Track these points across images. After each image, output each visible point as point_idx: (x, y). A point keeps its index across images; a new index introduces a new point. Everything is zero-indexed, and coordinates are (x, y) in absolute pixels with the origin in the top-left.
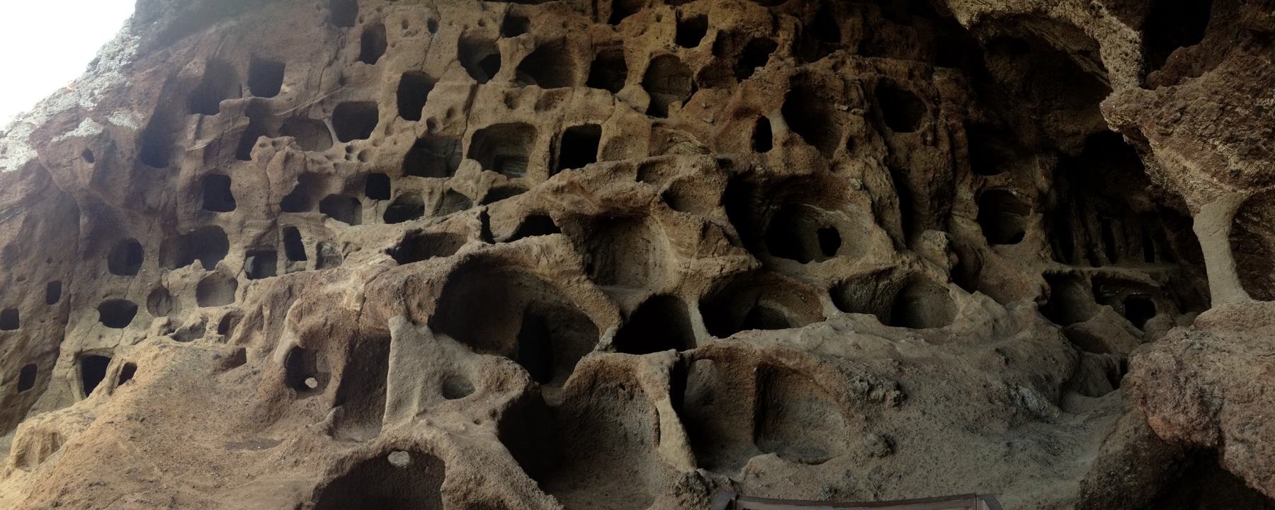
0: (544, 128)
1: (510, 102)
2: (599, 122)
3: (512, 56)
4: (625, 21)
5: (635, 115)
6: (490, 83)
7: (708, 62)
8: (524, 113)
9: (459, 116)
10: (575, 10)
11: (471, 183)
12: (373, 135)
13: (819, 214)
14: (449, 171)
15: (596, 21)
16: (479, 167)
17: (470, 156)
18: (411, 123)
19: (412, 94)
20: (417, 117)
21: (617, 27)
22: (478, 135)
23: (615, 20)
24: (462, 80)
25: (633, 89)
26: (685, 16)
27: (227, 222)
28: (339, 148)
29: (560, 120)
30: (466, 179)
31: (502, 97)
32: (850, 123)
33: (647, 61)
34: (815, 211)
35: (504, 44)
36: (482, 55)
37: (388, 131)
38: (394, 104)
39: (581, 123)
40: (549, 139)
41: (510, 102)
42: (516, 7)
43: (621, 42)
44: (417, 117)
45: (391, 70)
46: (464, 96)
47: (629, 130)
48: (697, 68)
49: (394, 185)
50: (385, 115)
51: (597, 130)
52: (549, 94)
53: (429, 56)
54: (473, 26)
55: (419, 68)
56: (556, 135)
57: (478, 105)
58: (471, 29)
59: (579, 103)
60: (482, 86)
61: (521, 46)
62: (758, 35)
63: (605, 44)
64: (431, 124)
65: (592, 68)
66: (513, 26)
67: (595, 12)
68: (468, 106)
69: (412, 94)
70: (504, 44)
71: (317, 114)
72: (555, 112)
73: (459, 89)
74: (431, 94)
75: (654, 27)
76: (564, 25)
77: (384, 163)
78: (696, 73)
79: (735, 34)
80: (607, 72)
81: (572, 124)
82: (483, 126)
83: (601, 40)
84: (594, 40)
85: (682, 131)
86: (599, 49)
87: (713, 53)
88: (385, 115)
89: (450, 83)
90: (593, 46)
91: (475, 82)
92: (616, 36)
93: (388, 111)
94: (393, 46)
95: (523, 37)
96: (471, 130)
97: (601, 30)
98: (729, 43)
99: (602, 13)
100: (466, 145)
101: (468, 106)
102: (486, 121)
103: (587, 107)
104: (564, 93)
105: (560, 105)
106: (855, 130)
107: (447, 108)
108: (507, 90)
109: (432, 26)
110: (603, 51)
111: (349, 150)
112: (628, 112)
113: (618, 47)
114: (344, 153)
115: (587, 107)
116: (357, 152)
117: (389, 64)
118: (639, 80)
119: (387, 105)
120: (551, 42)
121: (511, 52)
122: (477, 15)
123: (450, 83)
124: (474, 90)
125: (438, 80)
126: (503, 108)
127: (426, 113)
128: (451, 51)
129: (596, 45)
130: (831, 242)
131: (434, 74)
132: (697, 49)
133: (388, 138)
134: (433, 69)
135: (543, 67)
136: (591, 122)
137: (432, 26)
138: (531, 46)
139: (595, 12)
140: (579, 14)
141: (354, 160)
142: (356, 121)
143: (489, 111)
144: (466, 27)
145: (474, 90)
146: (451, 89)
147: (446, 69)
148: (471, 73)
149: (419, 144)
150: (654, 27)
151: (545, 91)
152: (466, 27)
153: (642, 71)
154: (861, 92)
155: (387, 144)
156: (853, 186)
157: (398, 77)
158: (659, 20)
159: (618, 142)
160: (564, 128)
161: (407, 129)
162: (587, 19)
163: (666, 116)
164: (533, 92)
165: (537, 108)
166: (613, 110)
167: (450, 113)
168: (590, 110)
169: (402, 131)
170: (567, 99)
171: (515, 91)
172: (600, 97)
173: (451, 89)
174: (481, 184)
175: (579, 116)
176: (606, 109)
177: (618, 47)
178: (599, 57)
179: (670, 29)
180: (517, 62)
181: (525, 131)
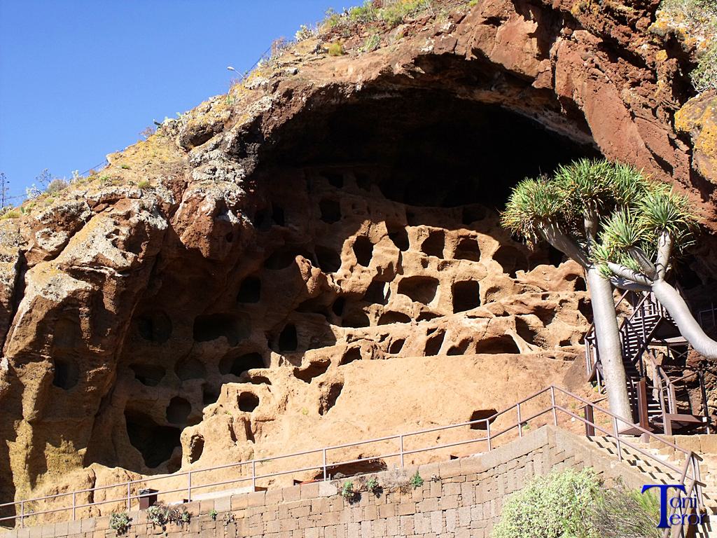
8: (431, 271)
18: (365, 268)
24: (391, 245)
41: (425, 264)
46: (397, 257)
47: (499, 284)
59: (463, 269)
60: (402, 252)
73: (393, 253)
77: (354, 290)
78: (527, 258)
85: (530, 286)
86: (461, 239)
89: (385, 248)
94: (345, 218)
96: (399, 278)
102: (408, 274)
126: (420, 266)
127: (373, 264)
136: (473, 279)
143: (412, 269)
147: (381, 239)
159: (493, 290)
164: (434, 261)
167: (391, 264)
169: (362, 272)
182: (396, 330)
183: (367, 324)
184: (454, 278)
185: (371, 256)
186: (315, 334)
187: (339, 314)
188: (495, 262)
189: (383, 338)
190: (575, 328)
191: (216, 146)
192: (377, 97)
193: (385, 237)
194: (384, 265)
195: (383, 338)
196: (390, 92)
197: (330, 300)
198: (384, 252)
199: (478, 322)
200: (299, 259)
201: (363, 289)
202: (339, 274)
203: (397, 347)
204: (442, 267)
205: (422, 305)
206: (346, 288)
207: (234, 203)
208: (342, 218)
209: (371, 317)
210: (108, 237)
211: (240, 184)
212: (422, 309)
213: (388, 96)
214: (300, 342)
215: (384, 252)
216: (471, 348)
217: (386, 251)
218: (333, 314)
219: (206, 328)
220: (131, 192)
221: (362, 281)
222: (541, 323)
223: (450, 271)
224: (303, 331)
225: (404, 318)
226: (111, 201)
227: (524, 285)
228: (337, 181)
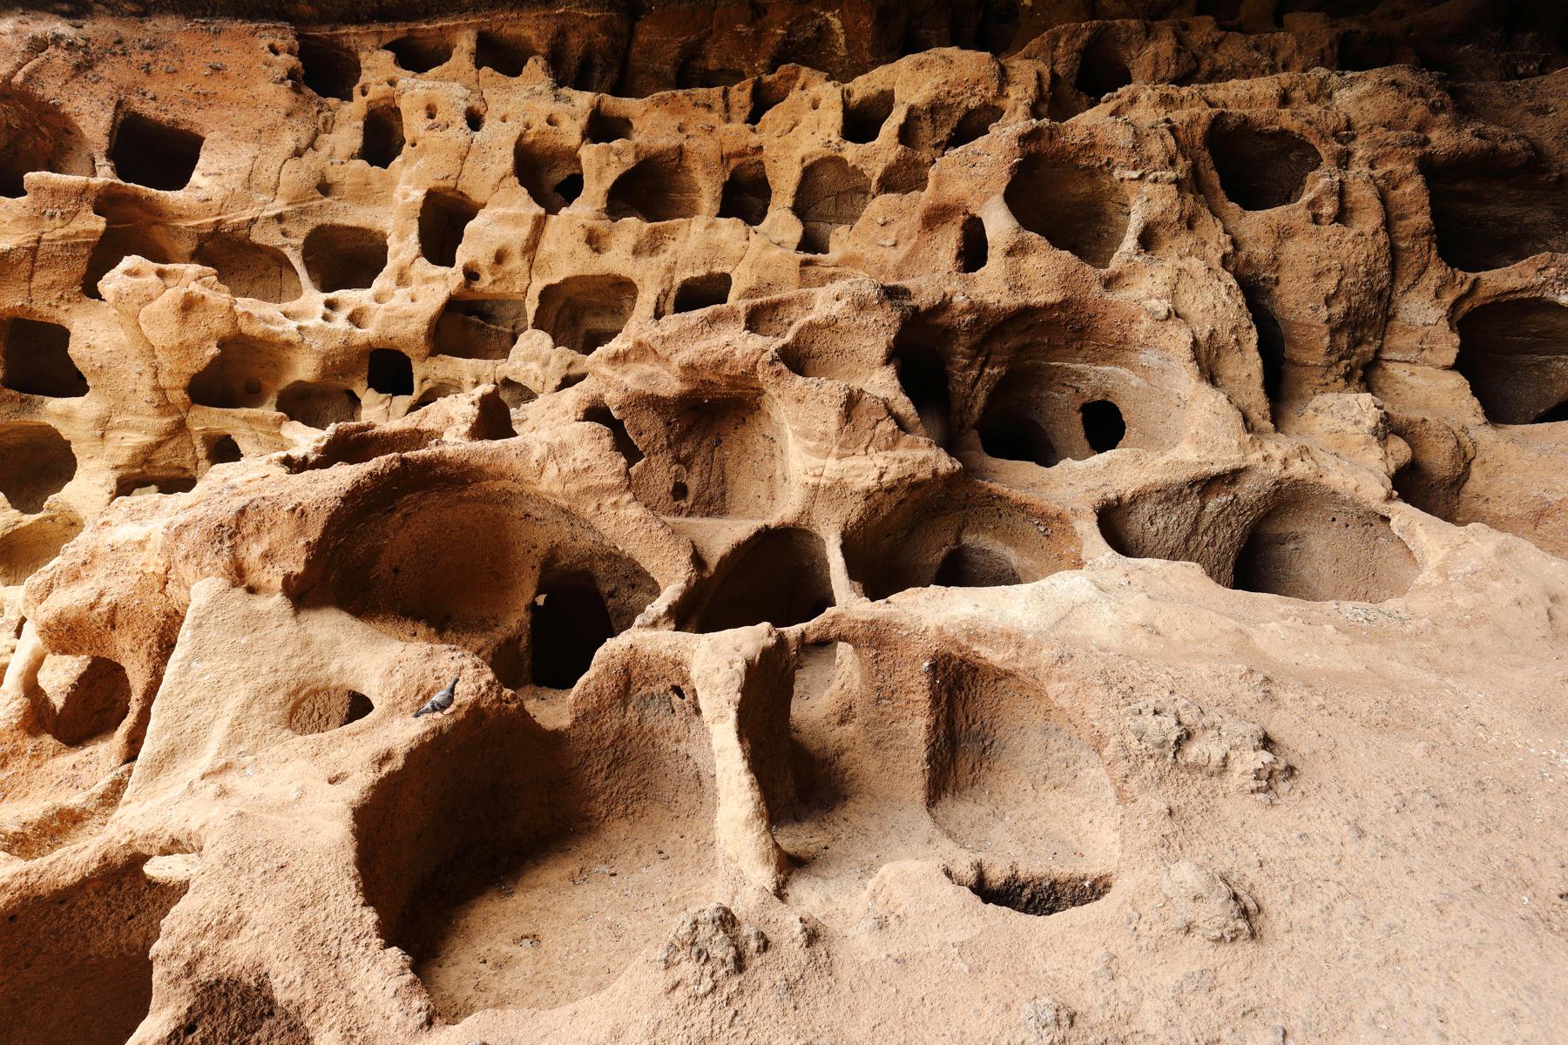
0: (647, 283)
1: (594, 241)
2: (727, 270)
3: (600, 172)
4: (767, 115)
5: (777, 252)
6: (564, 211)
7: (892, 158)
8: (616, 260)
9: (517, 263)
10: (695, 105)
11: (534, 367)
12: (377, 284)
13: (1080, 376)
14: (501, 346)
15: (728, 120)
16: (548, 340)
17: (539, 324)
19: (443, 223)
20: (451, 263)
21: (757, 127)
22: (547, 294)
23: (754, 119)
24: (523, 206)
25: (782, 223)
26: (856, 97)
28: (312, 298)
29: (670, 270)
30: (527, 359)
31: (581, 234)
32: (1146, 200)
33: (796, 173)
34: (1074, 372)
35: (589, 154)
36: (559, 175)
37: (402, 279)
38: (414, 237)
39: (701, 272)
40: (654, 299)
42: (609, 100)
43: (759, 149)
44: (451, 263)
45: (409, 182)
46: (525, 231)
47: (768, 276)
48: (875, 170)
49: (418, 371)
50: (397, 253)
52: (654, 231)
53: (467, 165)
54: (539, 124)
55: (450, 183)
56: (666, 294)
57: (547, 246)
58: (535, 128)
61: (614, 158)
62: (973, 103)
63: (741, 154)
64: (471, 274)
65: (724, 192)
66: (602, 128)
67: (727, 108)
68: (531, 246)
69: (443, 223)
70: (589, 154)
71: (265, 236)
72: (663, 259)
73: (516, 220)
74: (470, 226)
75: (808, 117)
76: (680, 130)
79: (935, 108)
80: (744, 197)
81: (688, 274)
82: (556, 280)
83: (734, 149)
84: (726, 151)
86: (733, 163)
87: (901, 142)
88: (397, 253)
89: (501, 211)
90: (725, 159)
91: (542, 211)
92: (754, 140)
93: (403, 247)
95: (617, 144)
96: (538, 286)
97: (736, 133)
98: (926, 127)
99: (735, 109)
100: (531, 307)
101: (531, 246)
103: (709, 247)
104: (675, 229)
105: (672, 246)
106: (1158, 209)
107: (494, 248)
108: (589, 224)
109: (474, 120)
110: (739, 167)
111: (331, 305)
112: (766, 247)
113: (757, 158)
114: (321, 309)
115: (709, 247)
116: (349, 311)
118: (789, 202)
119: (402, 237)
120: (660, 154)
121: (601, 167)
122: (546, 106)
123: (501, 211)
124: (539, 225)
125: (484, 205)
126: (584, 251)
127: (463, 255)
128: (505, 160)
129: (730, 156)
130: (1105, 426)
131: (476, 196)
132: (877, 142)
133: (401, 292)
134: (475, 185)
135: (648, 192)
136: (717, 269)
137: (474, 120)
138: (630, 160)
139: (727, 108)
140: (702, 111)
141: (340, 322)
142: (347, 260)
143: (565, 252)
144: (528, 127)
145: (539, 225)
146: (502, 220)
147: (496, 188)
148: (537, 195)
149: (455, 307)
150: (808, 117)
151: (647, 226)
152: (528, 127)
153: (791, 188)
154: (1171, 141)
156: (1152, 313)
157: (418, 195)
158: (815, 107)
160: (677, 281)
161: (433, 279)
162: (714, 118)
163: (826, 251)
164: (632, 227)
165: (637, 252)
166: (746, 249)
167: (500, 257)
168: (715, 249)
169: (427, 281)
170: (680, 238)
171: (603, 225)
172: (730, 228)
173: (502, 220)
174: (550, 369)
175: (699, 261)
176: (735, 247)
177: (757, 158)
178: (733, 174)
179: (832, 118)
180: (608, 183)
181: (619, 291)
190: (832, 467)
193: (507, 182)
208: (406, 147)
212: (570, 365)
227: (831, 270)
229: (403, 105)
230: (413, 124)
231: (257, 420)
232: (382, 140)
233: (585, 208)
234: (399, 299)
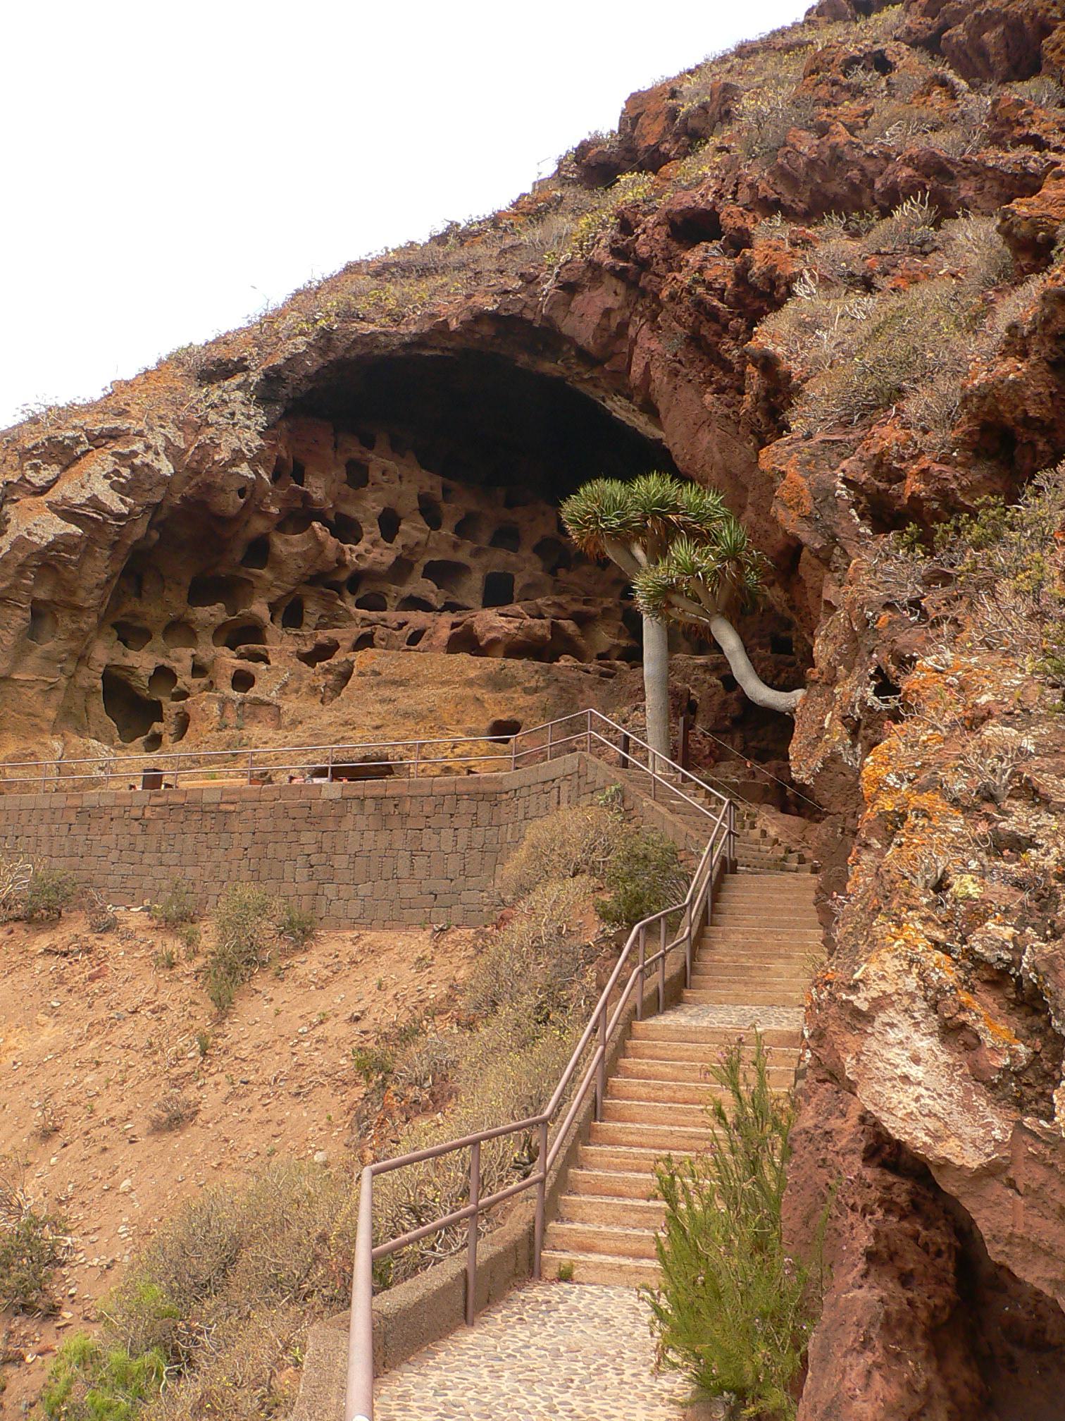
8: (462, 556)
24: (421, 523)
27: (259, 577)
37: (374, 543)
41: (456, 546)
51: (510, 579)
59: (499, 559)
69: (389, 524)
73: (421, 530)
96: (427, 559)
117: (371, 496)
127: (399, 540)
155: (375, 554)
157: (380, 509)
167: (417, 544)
171: (459, 542)
182: (417, 618)
183: (384, 609)
184: (487, 567)
185: (397, 531)
186: (324, 612)
187: (353, 593)
188: (535, 558)
189: (401, 626)
191: (239, 387)
192: (426, 353)
194: (411, 543)
195: (401, 626)
196: (443, 349)
197: (344, 576)
198: (412, 530)
199: (510, 622)
200: (316, 525)
201: (384, 568)
202: (360, 548)
203: (415, 638)
204: (476, 553)
205: (448, 594)
206: (363, 565)
207: (249, 455)
209: (391, 603)
210: (106, 477)
211: (260, 433)
213: (439, 353)
214: (307, 619)
215: (412, 530)
216: (500, 649)
217: (414, 528)
218: (347, 593)
219: (201, 593)
220: (138, 428)
221: (384, 559)
222: (578, 632)
223: (484, 559)
224: (312, 610)
225: (425, 606)
226: (114, 435)
228: (369, 444)
229: (372, 466)
230: (375, 474)
231: (322, 593)
232: (358, 476)
233: (446, 531)
234: (375, 554)
